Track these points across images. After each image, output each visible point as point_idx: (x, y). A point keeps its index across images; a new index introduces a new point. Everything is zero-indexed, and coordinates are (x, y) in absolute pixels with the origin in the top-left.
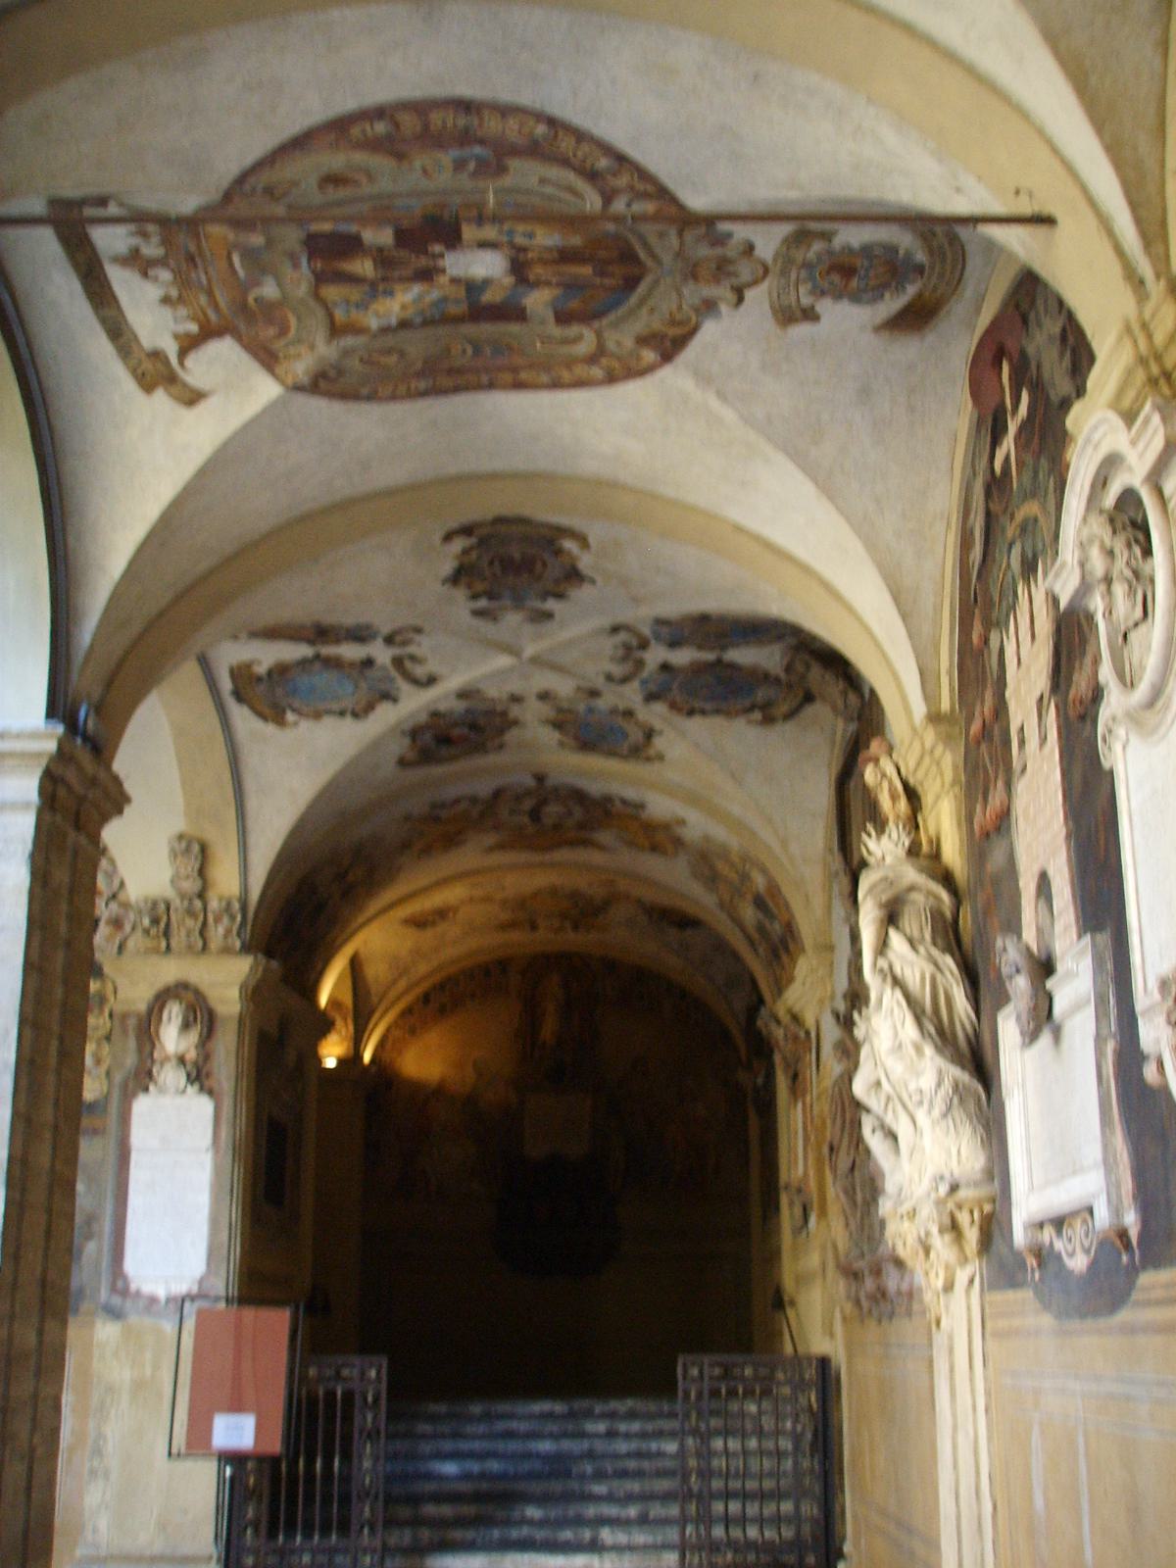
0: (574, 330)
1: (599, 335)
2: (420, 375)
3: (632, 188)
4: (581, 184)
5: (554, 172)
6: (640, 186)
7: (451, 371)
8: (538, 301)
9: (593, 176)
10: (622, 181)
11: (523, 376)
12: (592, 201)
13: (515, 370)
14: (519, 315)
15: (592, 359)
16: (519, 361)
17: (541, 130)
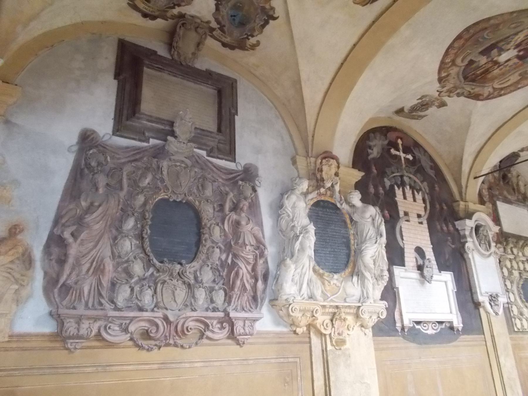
0: (466, 62)
1: (461, 67)
2: (498, 25)
3: (492, 94)
4: (503, 86)
5: (509, 83)
6: (492, 96)
7: (486, 29)
8: (483, 60)
9: (502, 89)
10: (496, 93)
11: (462, 41)
12: (496, 86)
13: (467, 40)
14: (483, 53)
15: (453, 62)
16: (469, 43)
17: (519, 86)
